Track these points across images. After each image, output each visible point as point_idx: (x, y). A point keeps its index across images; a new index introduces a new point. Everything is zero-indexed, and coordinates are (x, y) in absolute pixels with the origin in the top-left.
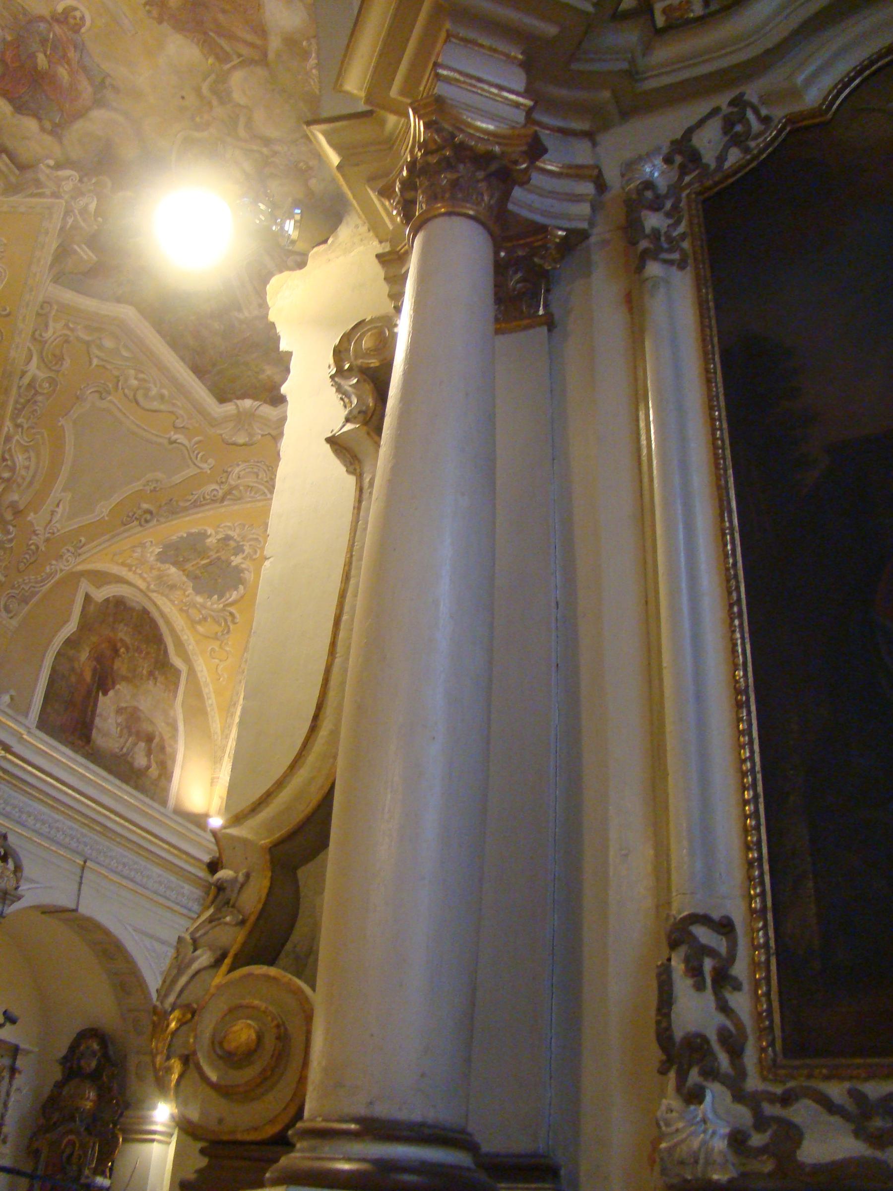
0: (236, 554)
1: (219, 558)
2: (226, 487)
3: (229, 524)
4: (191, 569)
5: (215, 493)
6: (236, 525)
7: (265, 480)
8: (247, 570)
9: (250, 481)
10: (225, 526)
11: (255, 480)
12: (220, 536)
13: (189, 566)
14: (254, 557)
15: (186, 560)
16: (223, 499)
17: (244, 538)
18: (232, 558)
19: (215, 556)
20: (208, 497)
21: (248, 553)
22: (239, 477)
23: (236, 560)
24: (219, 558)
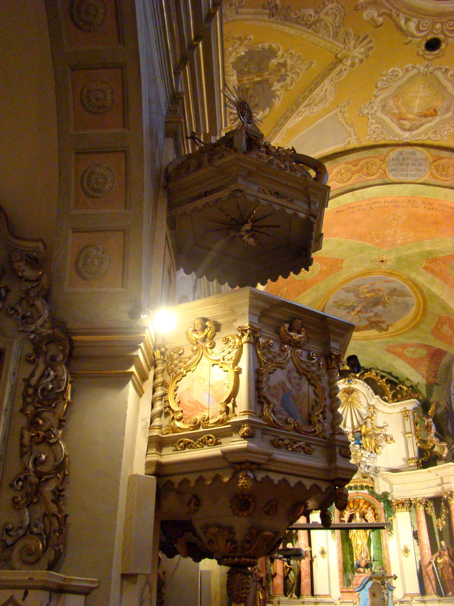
0: (279, 81)
1: (267, 80)
2: (317, 17)
3: (294, 52)
4: (246, 82)
5: (310, 18)
6: (296, 55)
7: (337, 25)
8: (278, 97)
9: (329, 20)
10: (291, 54)
11: (332, 21)
12: (282, 61)
13: (245, 80)
14: (289, 88)
15: (249, 73)
16: (310, 27)
17: (293, 67)
18: (275, 83)
19: (266, 77)
20: (305, 19)
21: (287, 84)
22: (326, 14)
23: (276, 86)
24: (267, 80)
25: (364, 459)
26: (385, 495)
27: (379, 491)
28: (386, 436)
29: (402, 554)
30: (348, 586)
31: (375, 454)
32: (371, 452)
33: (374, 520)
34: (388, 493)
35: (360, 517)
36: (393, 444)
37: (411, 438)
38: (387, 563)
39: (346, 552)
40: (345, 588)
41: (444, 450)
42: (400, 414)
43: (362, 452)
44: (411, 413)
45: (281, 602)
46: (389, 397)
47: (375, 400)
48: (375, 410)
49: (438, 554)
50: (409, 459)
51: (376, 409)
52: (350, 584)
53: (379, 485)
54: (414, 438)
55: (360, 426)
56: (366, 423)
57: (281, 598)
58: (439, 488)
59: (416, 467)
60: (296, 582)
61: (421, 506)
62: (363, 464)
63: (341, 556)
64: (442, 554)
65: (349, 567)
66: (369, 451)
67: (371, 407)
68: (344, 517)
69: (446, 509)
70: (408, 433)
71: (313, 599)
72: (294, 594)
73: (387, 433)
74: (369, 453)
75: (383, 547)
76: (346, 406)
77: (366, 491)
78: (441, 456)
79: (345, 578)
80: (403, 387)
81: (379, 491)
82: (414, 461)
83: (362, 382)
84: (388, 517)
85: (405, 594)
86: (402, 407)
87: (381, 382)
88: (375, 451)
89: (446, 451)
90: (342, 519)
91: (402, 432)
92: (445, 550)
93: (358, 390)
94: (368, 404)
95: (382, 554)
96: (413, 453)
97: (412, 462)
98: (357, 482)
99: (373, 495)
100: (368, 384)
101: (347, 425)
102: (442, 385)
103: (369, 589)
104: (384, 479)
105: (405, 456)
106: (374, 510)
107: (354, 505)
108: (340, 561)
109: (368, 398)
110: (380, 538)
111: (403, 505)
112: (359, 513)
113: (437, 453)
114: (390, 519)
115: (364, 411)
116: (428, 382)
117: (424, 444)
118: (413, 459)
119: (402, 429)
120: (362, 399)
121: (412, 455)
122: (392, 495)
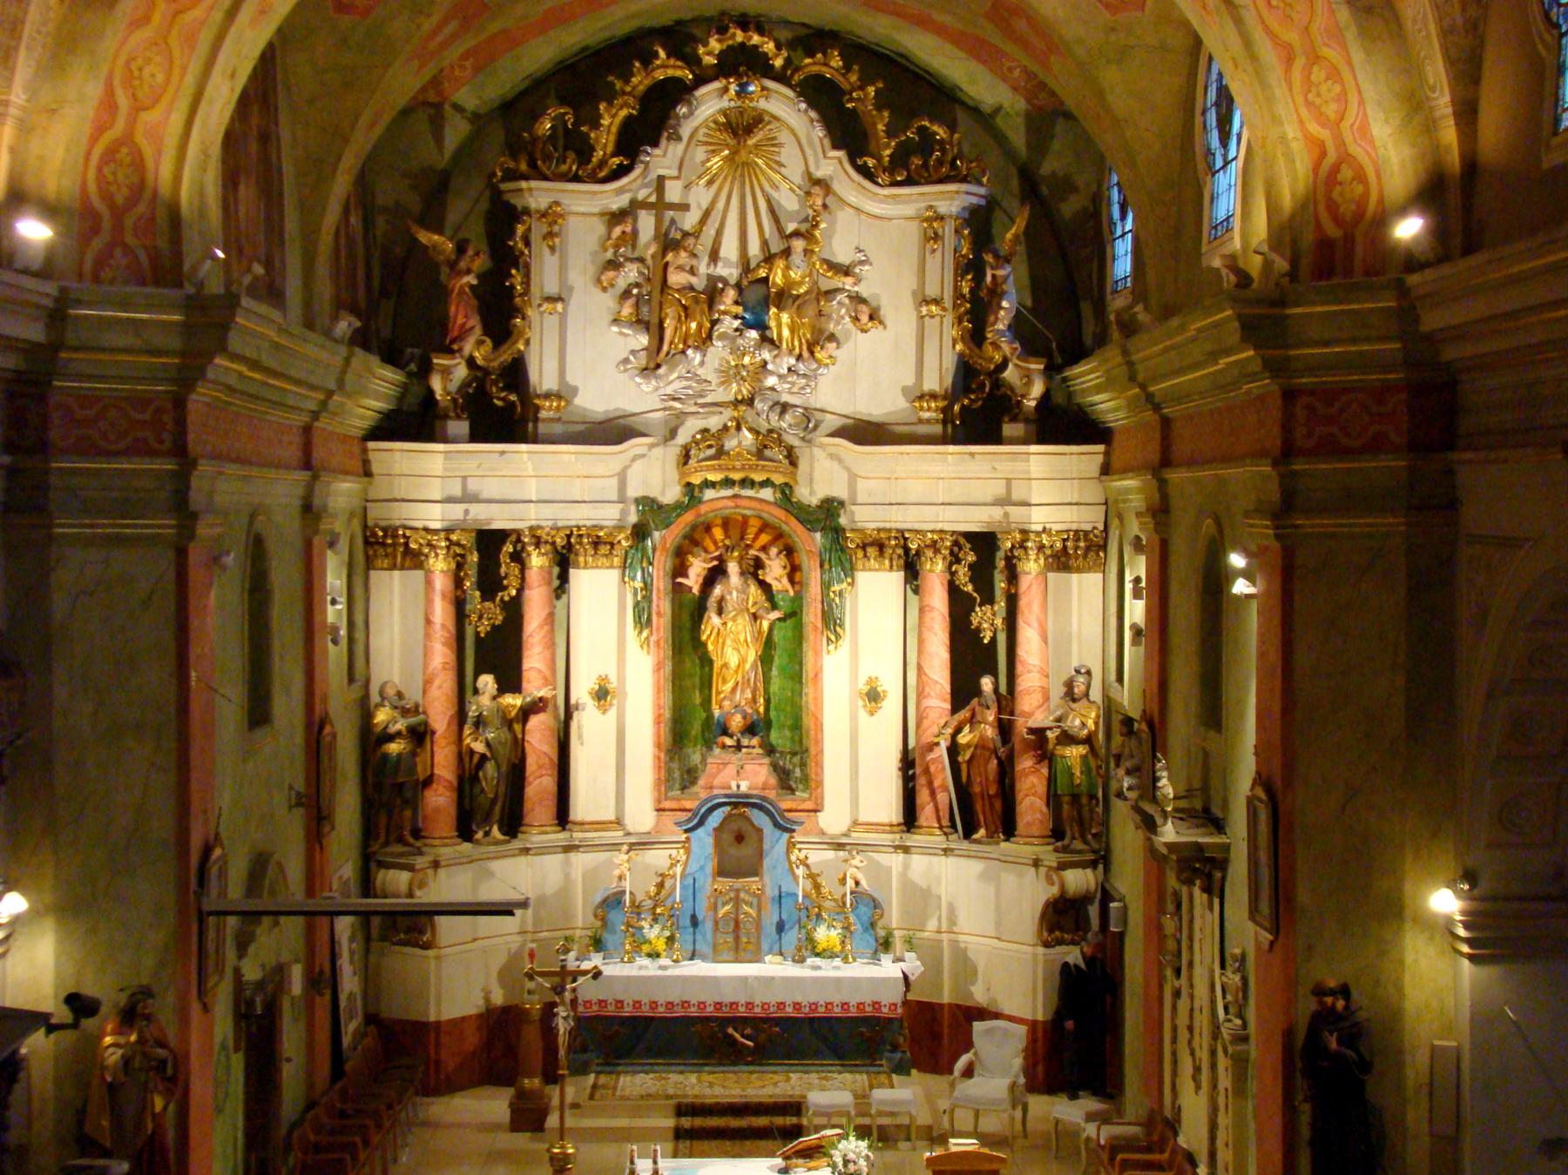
25: (771, 381)
26: (830, 509)
27: (809, 494)
28: (858, 299)
29: (861, 703)
30: (683, 788)
31: (814, 366)
32: (799, 358)
33: (789, 586)
34: (842, 504)
35: (742, 574)
36: (876, 333)
38: (812, 726)
39: (688, 683)
40: (674, 799)
41: (1029, 384)
44: (948, 230)
45: (443, 863)
46: (879, 159)
47: (832, 165)
48: (829, 201)
50: (921, 397)
51: (835, 194)
52: (694, 782)
53: (816, 475)
54: (949, 319)
55: (769, 259)
56: (787, 253)
57: (443, 850)
58: (996, 513)
59: (938, 429)
60: (502, 790)
62: (762, 401)
63: (667, 699)
64: (979, 717)
65: (696, 728)
66: (791, 351)
67: (817, 190)
68: (686, 576)
70: (927, 302)
71: (561, 837)
72: (495, 828)
73: (863, 290)
74: (792, 361)
76: (725, 178)
77: (767, 494)
78: (1019, 403)
79: (675, 765)
80: (935, 128)
81: (812, 493)
82: (933, 405)
83: (790, 93)
85: (855, 823)
86: (923, 205)
87: (859, 99)
88: (812, 353)
89: (1037, 389)
90: (679, 580)
91: (914, 293)
92: (988, 708)
93: (776, 118)
94: (809, 174)
96: (938, 374)
97: (929, 409)
98: (734, 469)
99: (788, 506)
100: (812, 104)
101: (722, 254)
103: (715, 830)
105: (910, 380)
106: (789, 551)
107: (727, 536)
108: (660, 716)
109: (808, 151)
110: (800, 644)
111: (881, 547)
112: (741, 560)
113: (1012, 389)
115: (789, 202)
116: (1033, 106)
117: (977, 350)
118: (933, 396)
120: (789, 154)
121: (932, 383)
122: (853, 513)
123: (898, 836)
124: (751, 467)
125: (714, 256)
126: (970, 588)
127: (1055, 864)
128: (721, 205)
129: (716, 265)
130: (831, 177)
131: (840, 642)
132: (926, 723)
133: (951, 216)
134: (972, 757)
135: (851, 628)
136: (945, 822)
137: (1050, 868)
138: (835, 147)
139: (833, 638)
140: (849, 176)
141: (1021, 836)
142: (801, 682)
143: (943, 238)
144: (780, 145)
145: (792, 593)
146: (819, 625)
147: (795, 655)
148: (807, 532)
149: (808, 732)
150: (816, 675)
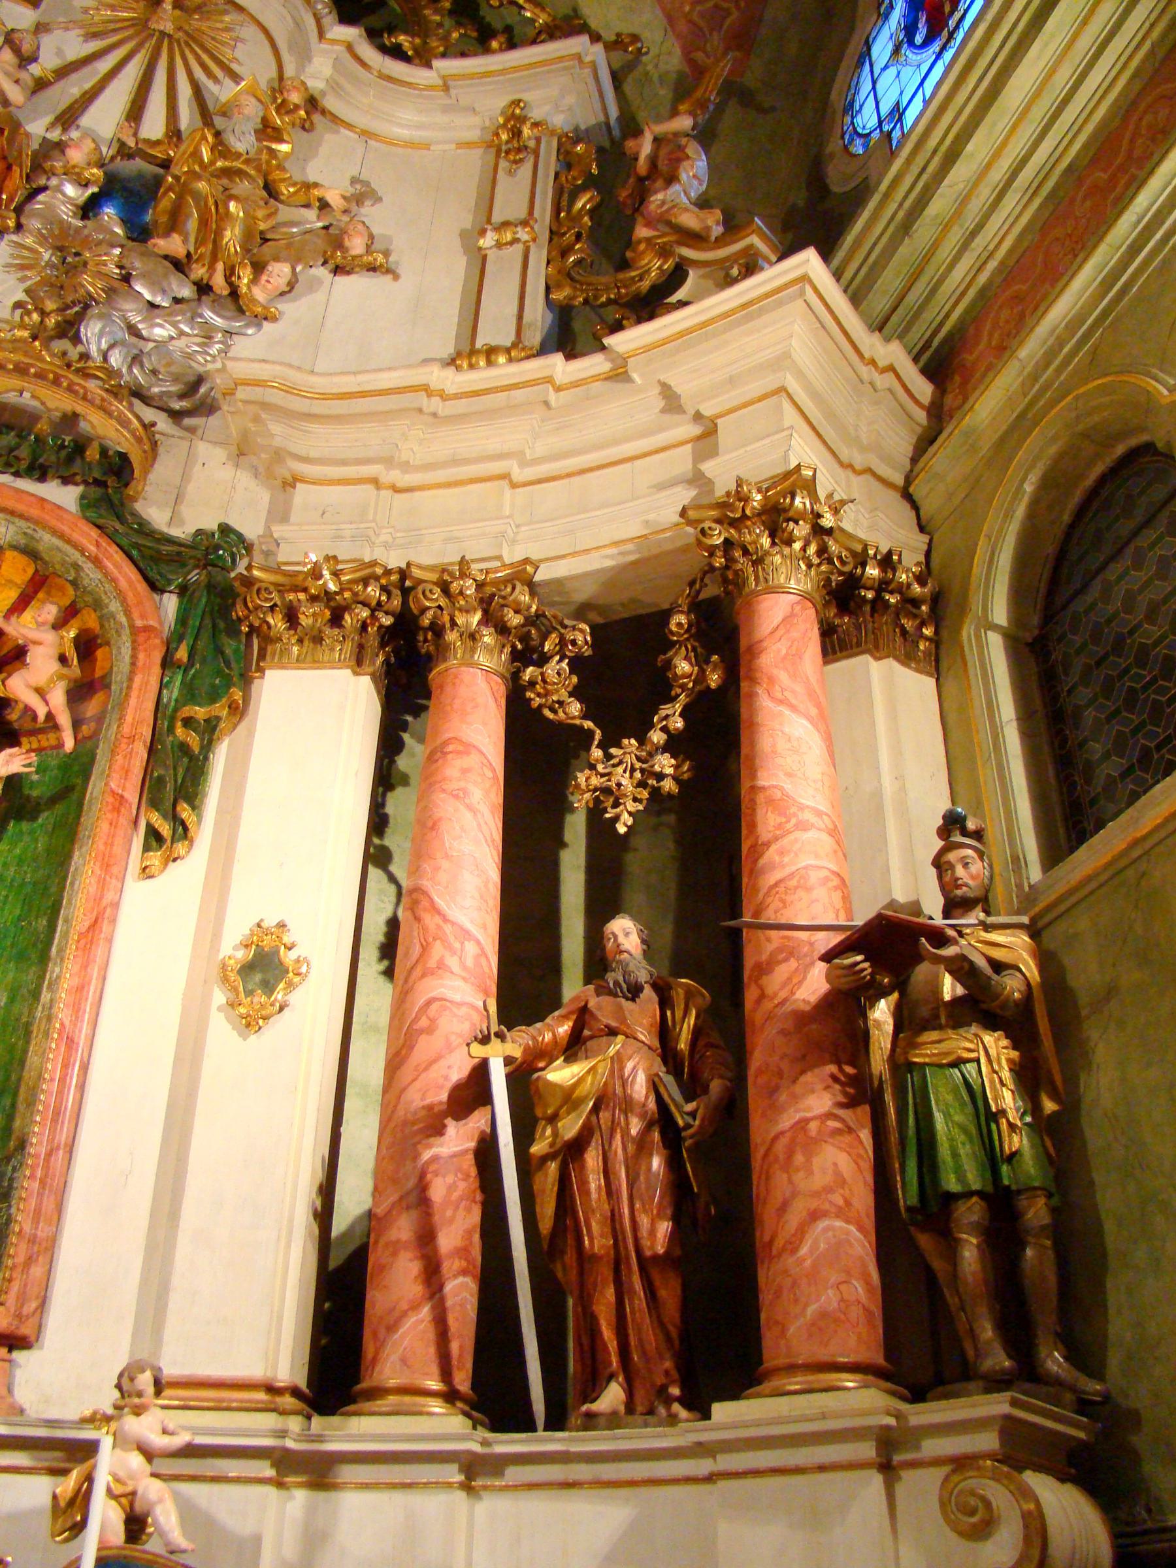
29: (219, 997)
32: (203, 289)
33: (64, 719)
37: (519, 247)
38: (53, 1068)
42: (478, 152)
43: (137, 264)
49: (564, 1029)
51: (324, 112)
53: (191, 488)
54: (539, 257)
61: (488, 637)
69: (701, 662)
74: (187, 292)
75: (66, 935)
84: (190, 694)
86: (502, 102)
88: (234, 294)
92: (634, 992)
95: (36, 995)
99: (113, 524)
101: (86, 121)
102: (773, 109)
104: (241, 452)
114: (200, 712)
116: (691, 62)
119: (471, 217)
123: (295, 1424)
124: (40, 375)
125: (68, 118)
126: (575, 708)
127: (988, 1441)
128: (104, 65)
129: (65, 130)
130: (323, 93)
131: (180, 848)
132: (424, 1048)
133: (552, 133)
134: (574, 1150)
135: (220, 811)
136: (463, 1381)
137: (961, 1463)
138: (346, 18)
139: (165, 829)
140: (363, 64)
141: (792, 1369)
142: (44, 958)
143: (536, 153)
144: (237, 40)
145: (69, 744)
146: (132, 796)
147: (45, 892)
148: (142, 586)
149: (34, 1091)
150: (95, 924)
